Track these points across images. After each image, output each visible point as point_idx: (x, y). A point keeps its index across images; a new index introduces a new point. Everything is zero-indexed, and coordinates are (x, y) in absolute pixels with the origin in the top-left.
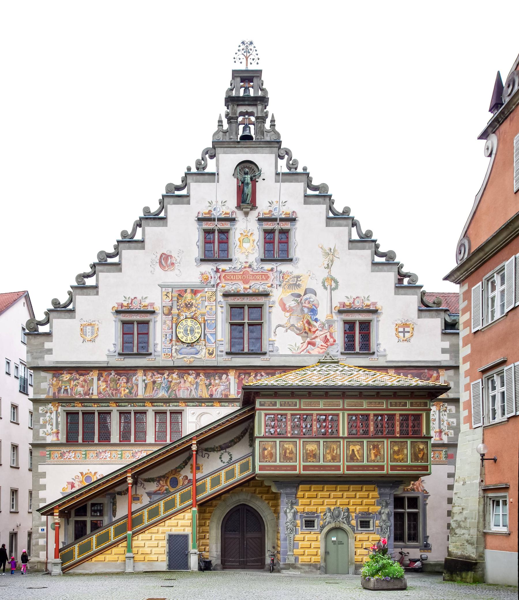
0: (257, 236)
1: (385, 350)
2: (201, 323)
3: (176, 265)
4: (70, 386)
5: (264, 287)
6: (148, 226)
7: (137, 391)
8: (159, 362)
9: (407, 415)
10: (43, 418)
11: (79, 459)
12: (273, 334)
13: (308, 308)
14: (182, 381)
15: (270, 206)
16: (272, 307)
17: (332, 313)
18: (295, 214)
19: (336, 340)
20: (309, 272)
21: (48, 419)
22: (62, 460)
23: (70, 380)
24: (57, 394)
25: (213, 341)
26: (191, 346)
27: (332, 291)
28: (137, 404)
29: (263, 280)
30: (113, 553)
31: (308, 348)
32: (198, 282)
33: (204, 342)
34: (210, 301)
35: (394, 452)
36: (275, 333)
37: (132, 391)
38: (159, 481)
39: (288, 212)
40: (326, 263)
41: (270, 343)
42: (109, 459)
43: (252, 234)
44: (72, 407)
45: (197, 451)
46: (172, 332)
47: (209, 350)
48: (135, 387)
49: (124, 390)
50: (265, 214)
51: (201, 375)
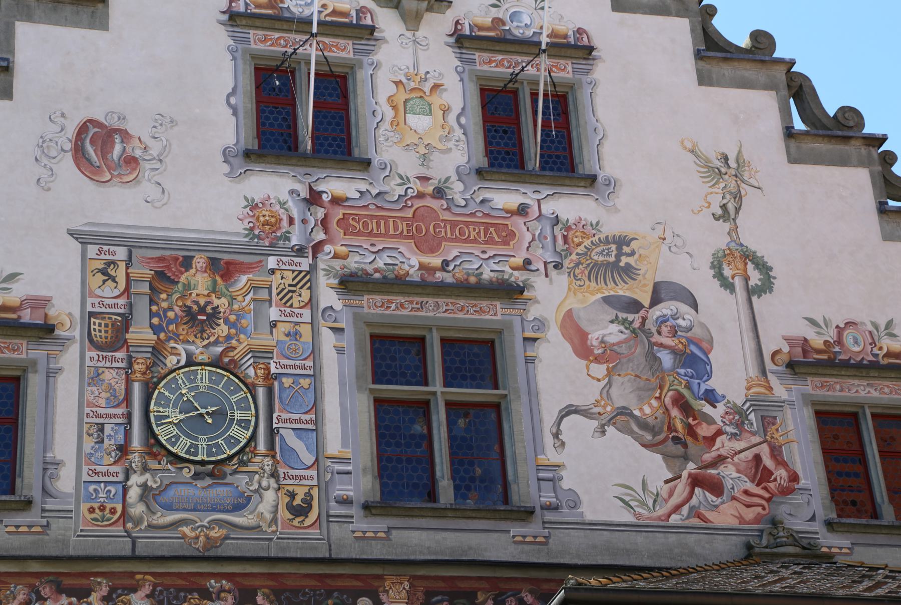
2: (254, 386)
5: (496, 267)
12: (549, 440)
13: (673, 351)
16: (535, 340)
17: (764, 372)
18: (585, 39)
20: (661, 227)
25: (309, 459)
26: (211, 475)
27: (754, 299)
29: (490, 241)
31: (694, 501)
32: (237, 234)
33: (268, 461)
36: (556, 435)
39: (561, 28)
40: (716, 201)
41: (541, 475)
43: (436, 87)
46: (129, 416)
47: (292, 495)
50: (481, 28)
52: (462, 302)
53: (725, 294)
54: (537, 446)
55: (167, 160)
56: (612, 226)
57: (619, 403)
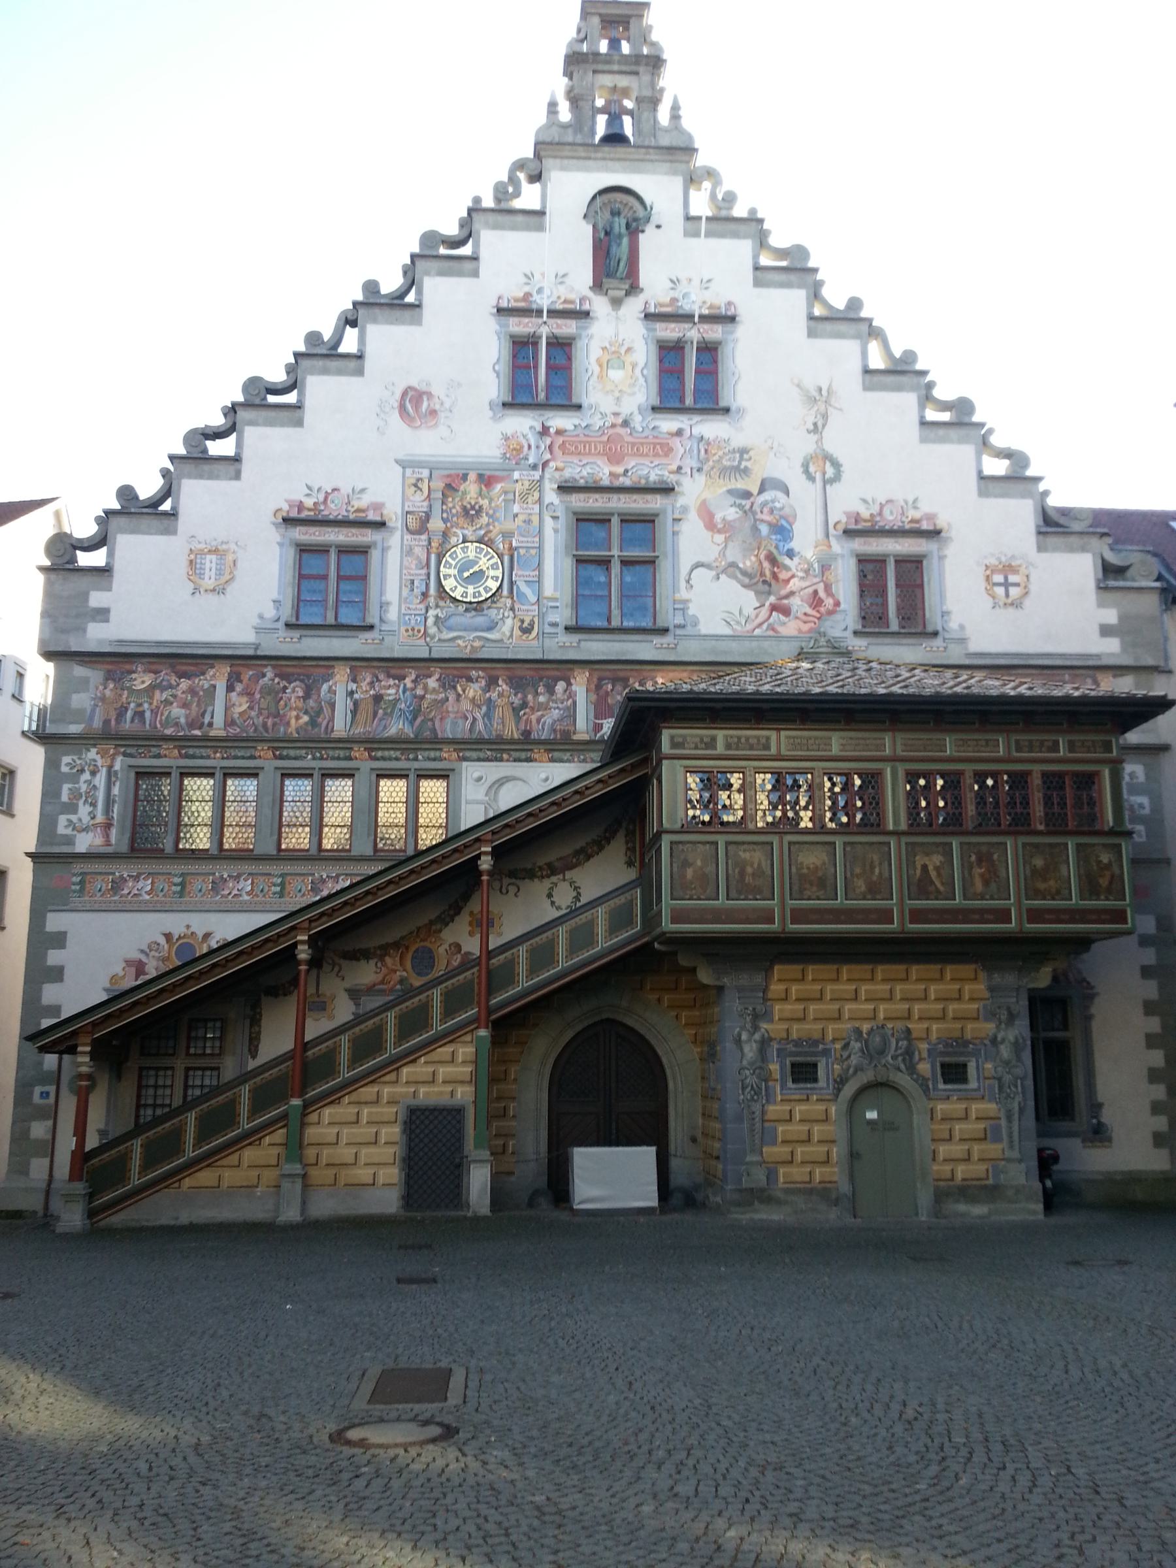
0: (643, 355)
1: (962, 627)
3: (442, 415)
4: (151, 704)
6: (375, 321)
7: (332, 719)
8: (392, 649)
9: (1061, 775)
10: (70, 786)
11: (164, 896)
12: (683, 584)
13: (770, 524)
14: (452, 697)
15: (672, 289)
17: (827, 536)
19: (842, 601)
22: (116, 898)
23: (152, 688)
24: (113, 722)
25: (533, 599)
26: (475, 610)
27: (828, 487)
28: (331, 753)
29: (656, 455)
30: (245, 1163)
31: (771, 620)
35: (1034, 871)
36: (688, 581)
37: (320, 720)
39: (716, 302)
40: (810, 420)
42: (246, 898)
43: (629, 350)
44: (155, 757)
45: (490, 873)
46: (428, 575)
47: (522, 621)
48: (327, 711)
49: (298, 718)
50: (662, 305)
51: (500, 682)
53: (809, 484)
54: (675, 588)
56: (738, 441)
57: (730, 559)
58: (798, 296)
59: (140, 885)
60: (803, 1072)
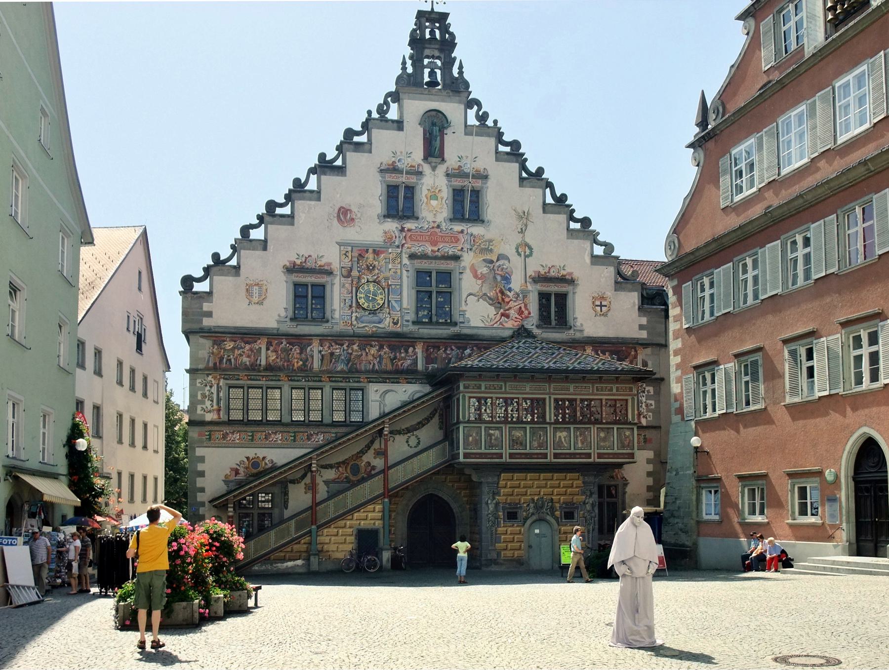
0: (446, 193)
1: (582, 325)
3: (357, 221)
4: (234, 356)
7: (312, 363)
12: (463, 303)
14: (364, 354)
15: (459, 161)
17: (526, 282)
21: (207, 393)
23: (234, 348)
24: (218, 364)
25: (398, 309)
26: (373, 313)
27: (527, 259)
28: (312, 378)
29: (452, 242)
31: (501, 320)
33: (388, 310)
34: (394, 262)
36: (465, 302)
38: (337, 468)
40: (520, 227)
42: (280, 442)
43: (440, 190)
46: (352, 297)
47: (394, 319)
48: (310, 359)
49: (297, 362)
50: (455, 170)
51: (385, 347)
52: (442, 262)
55: (362, 219)
56: (488, 236)
57: (484, 292)
58: (516, 166)
59: (234, 436)
60: (512, 516)
